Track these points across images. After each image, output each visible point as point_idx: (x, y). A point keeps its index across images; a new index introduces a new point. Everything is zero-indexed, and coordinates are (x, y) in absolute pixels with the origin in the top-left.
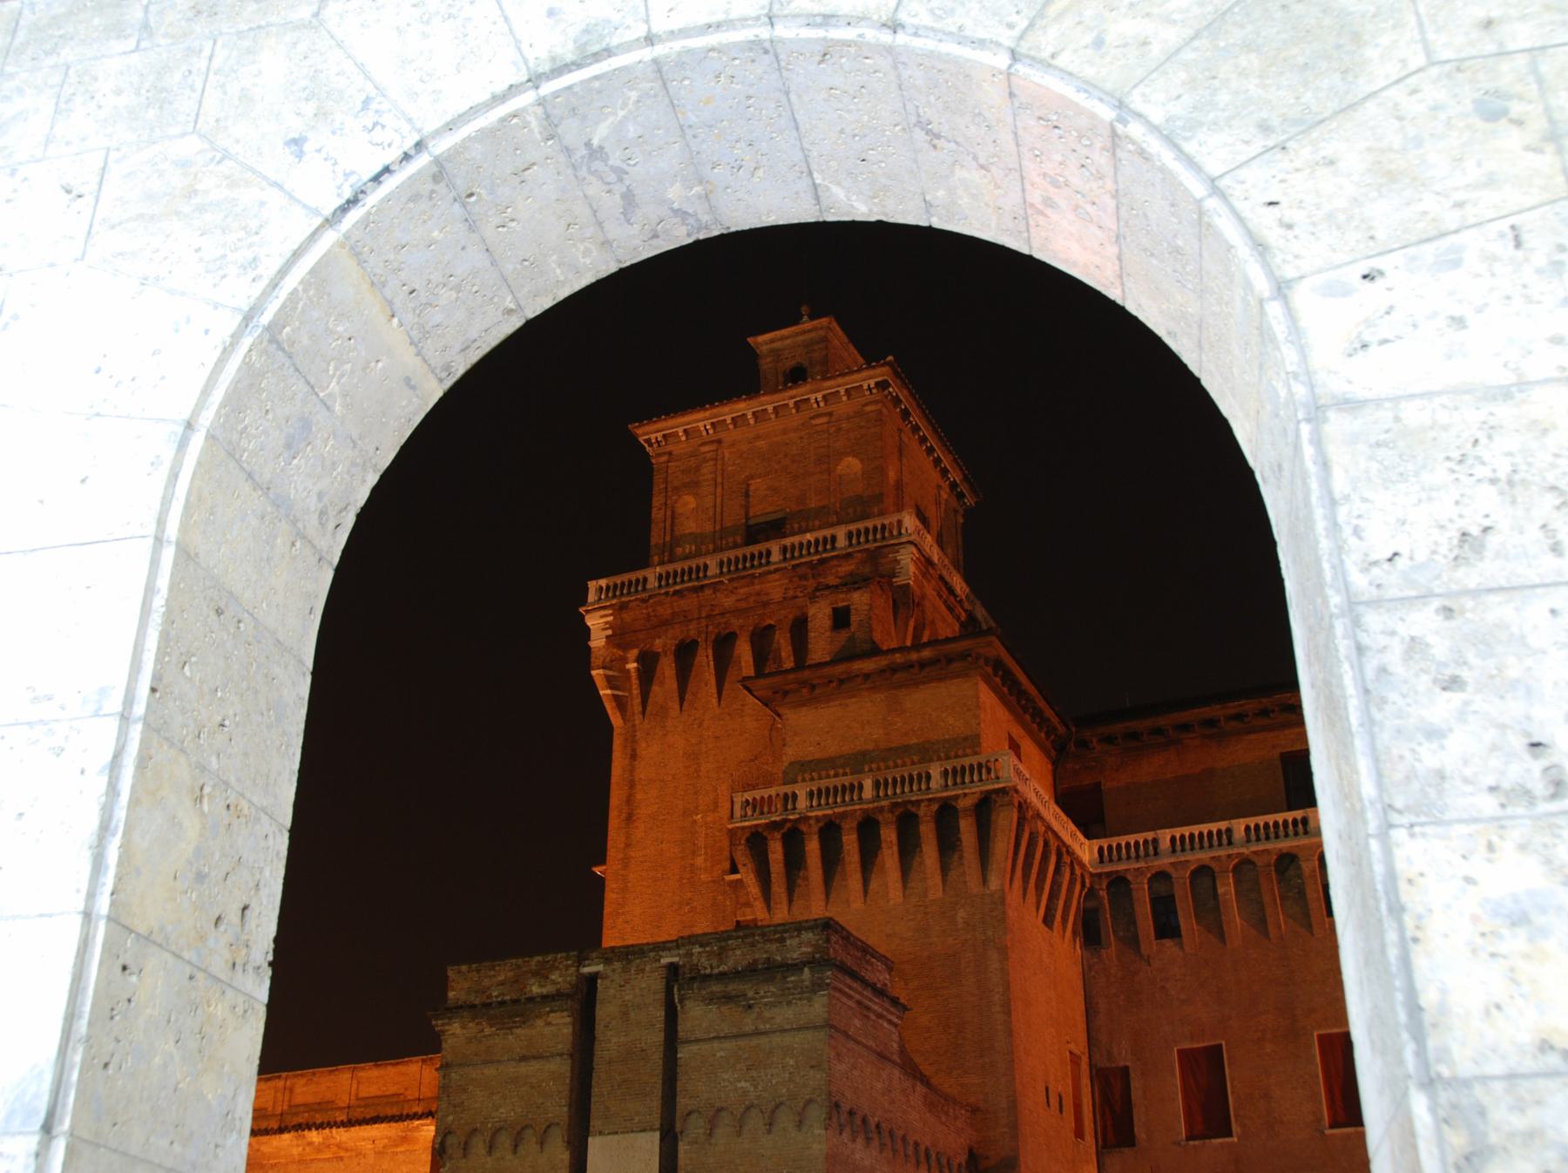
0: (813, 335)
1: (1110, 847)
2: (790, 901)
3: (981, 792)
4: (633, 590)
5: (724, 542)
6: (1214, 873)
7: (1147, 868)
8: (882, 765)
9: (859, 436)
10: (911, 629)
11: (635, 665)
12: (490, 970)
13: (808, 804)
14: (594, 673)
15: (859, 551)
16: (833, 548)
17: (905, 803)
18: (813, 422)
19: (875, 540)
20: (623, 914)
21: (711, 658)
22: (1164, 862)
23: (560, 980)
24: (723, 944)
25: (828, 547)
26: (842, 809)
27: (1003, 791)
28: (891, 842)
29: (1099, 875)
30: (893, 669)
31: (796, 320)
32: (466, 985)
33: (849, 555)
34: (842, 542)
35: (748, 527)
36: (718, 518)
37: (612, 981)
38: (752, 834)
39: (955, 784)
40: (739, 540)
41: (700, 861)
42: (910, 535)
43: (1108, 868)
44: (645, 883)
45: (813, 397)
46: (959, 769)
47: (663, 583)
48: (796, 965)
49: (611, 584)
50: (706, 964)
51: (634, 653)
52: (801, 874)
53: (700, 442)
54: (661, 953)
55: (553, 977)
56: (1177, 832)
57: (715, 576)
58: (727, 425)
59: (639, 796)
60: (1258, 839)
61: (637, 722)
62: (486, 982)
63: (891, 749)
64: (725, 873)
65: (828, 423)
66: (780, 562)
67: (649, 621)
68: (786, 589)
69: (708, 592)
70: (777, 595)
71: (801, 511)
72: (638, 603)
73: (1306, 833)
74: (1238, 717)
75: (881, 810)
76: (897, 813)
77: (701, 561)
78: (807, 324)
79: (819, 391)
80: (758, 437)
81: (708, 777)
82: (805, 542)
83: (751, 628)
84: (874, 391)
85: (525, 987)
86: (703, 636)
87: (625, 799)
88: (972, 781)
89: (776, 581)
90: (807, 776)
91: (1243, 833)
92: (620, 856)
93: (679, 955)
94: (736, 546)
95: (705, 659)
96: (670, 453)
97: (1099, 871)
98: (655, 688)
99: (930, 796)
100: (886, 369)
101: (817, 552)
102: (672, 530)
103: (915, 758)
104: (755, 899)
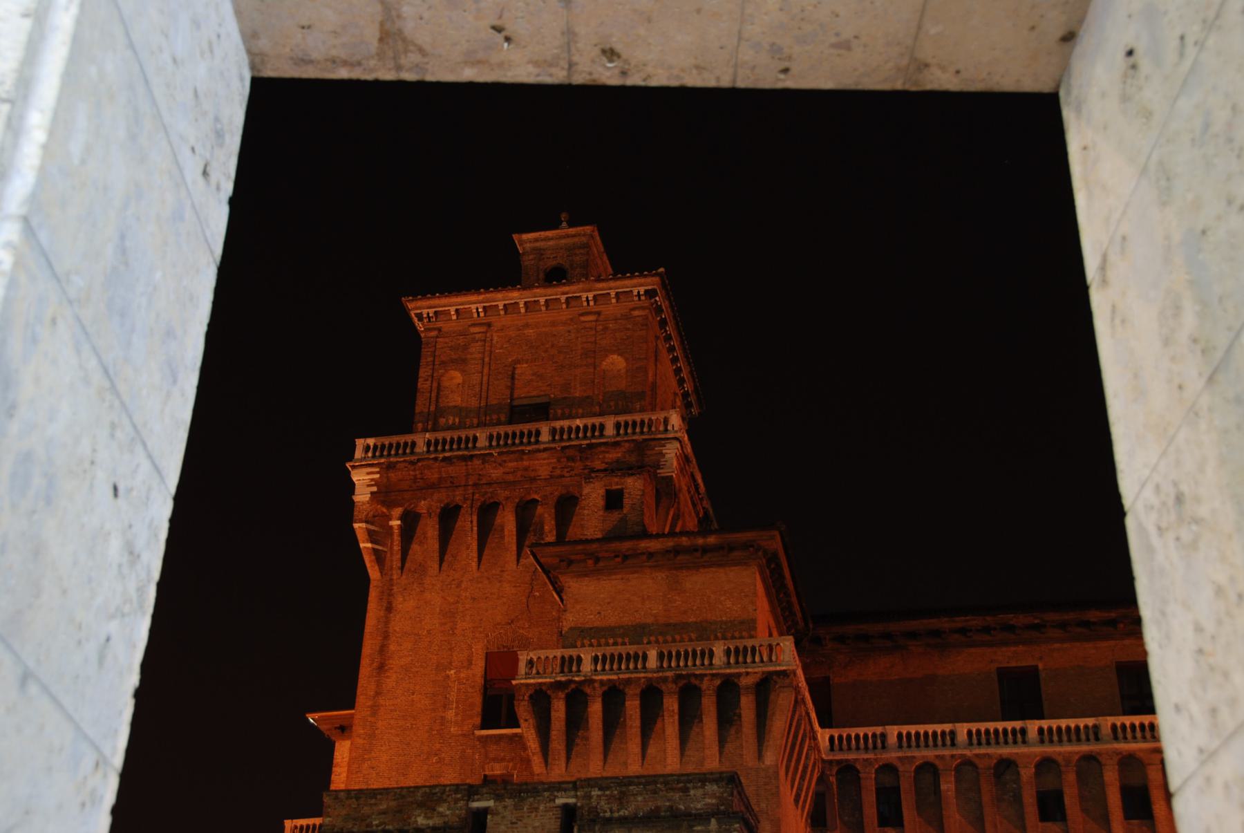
0: (576, 240)
1: (840, 737)
2: (568, 758)
3: (763, 673)
4: (400, 451)
5: (488, 418)
6: (898, 771)
7: (876, 760)
8: (661, 639)
9: (625, 337)
10: (670, 517)
11: (399, 522)
12: (371, 798)
13: (593, 668)
14: (356, 526)
15: (626, 441)
16: (602, 435)
17: (688, 676)
18: (582, 319)
19: (642, 433)
20: (369, 759)
21: (475, 523)
22: (892, 755)
23: (448, 812)
24: (624, 789)
25: (597, 434)
26: (627, 676)
27: (784, 674)
28: (673, 711)
29: (831, 762)
30: (677, 551)
31: (555, 225)
32: (344, 812)
33: (617, 444)
34: (610, 431)
35: (512, 408)
36: (484, 394)
37: (503, 817)
38: (610, 689)
39: (737, 662)
40: (503, 419)
41: (450, 715)
42: (676, 432)
43: (839, 756)
44: (393, 731)
45: (584, 296)
46: (741, 649)
47: (432, 449)
48: (700, 815)
49: (379, 444)
50: (606, 808)
51: (398, 511)
52: (579, 734)
53: (470, 323)
54: (556, 793)
55: (441, 809)
56: (905, 729)
57: (485, 448)
58: (499, 310)
59: (392, 647)
60: (979, 743)
61: (395, 577)
62: (366, 810)
63: (669, 625)
64: (475, 727)
65: (596, 321)
66: (549, 442)
67: (415, 482)
68: (553, 468)
69: (477, 462)
70: (544, 472)
71: (565, 398)
72: (406, 465)
73: (1024, 742)
74: (963, 631)
75: (665, 680)
76: (680, 684)
77: (471, 433)
78: (565, 230)
79: (590, 291)
80: (527, 326)
81: (464, 636)
82: (574, 427)
83: (517, 500)
84: (643, 298)
85: (409, 818)
86: (469, 502)
87: (378, 648)
88: (754, 662)
89: (544, 459)
90: (586, 642)
91: (896, 739)
92: (370, 703)
93: (576, 796)
94: (499, 423)
95: (468, 524)
96: (439, 330)
97: (831, 758)
98: (415, 547)
99: (714, 672)
100: (657, 279)
101: (585, 437)
102: (437, 401)
103: (693, 636)
104: (534, 754)
